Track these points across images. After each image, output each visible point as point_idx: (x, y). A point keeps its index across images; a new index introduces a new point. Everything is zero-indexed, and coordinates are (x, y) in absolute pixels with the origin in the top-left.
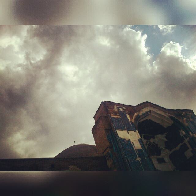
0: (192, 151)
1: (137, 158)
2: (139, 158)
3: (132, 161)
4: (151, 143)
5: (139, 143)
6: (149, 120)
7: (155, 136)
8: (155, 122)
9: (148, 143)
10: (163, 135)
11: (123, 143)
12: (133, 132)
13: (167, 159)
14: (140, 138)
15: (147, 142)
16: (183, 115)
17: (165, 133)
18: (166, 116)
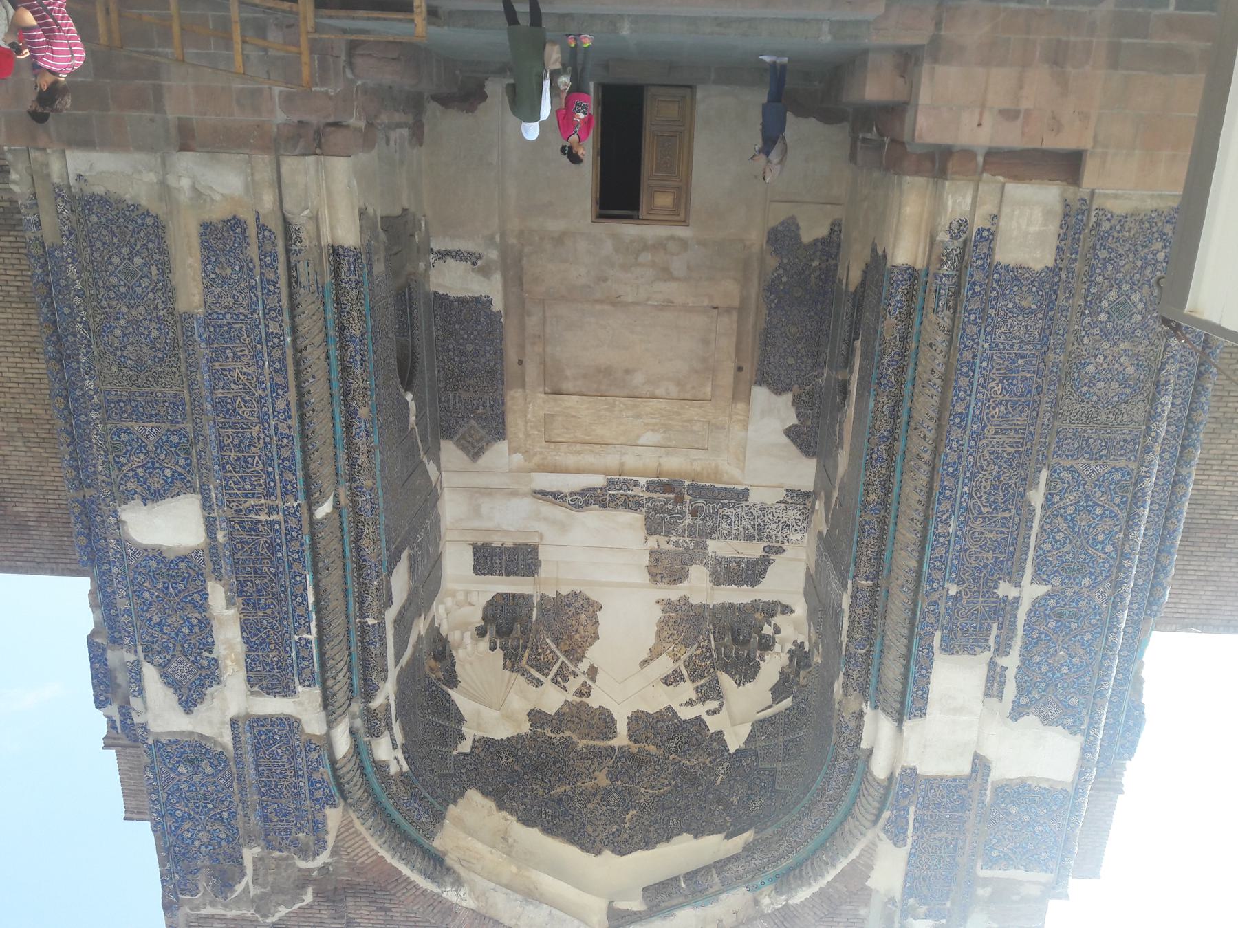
0: (389, 603)
1: (1035, 602)
2: (1017, 600)
3: (1087, 582)
4: (556, 683)
5: (933, 695)
6: (598, 853)
7: (526, 728)
8: (549, 830)
9: (574, 684)
10: (479, 735)
11: (1074, 701)
12: (929, 767)
13: (456, 562)
14: (878, 732)
15: (584, 692)
16: (310, 891)
17: (465, 747)
18: (482, 883)
